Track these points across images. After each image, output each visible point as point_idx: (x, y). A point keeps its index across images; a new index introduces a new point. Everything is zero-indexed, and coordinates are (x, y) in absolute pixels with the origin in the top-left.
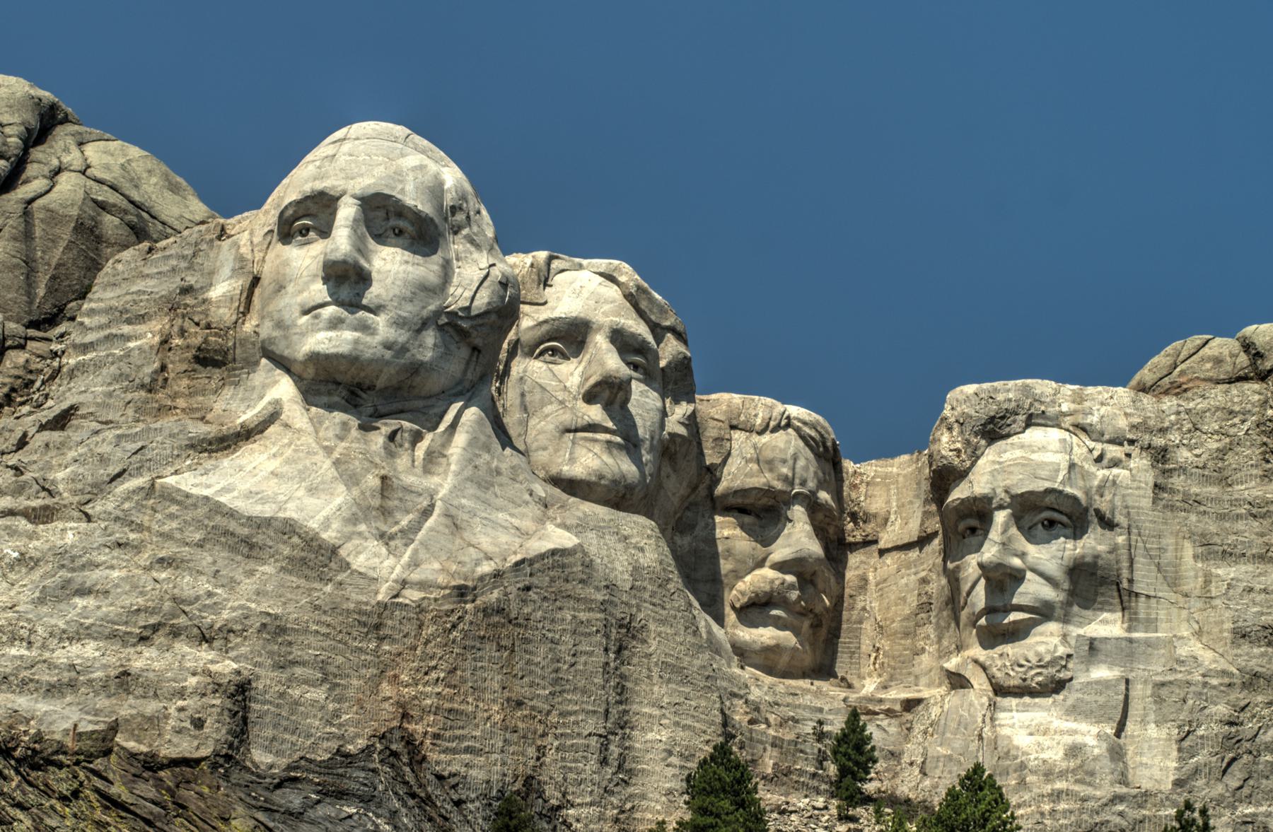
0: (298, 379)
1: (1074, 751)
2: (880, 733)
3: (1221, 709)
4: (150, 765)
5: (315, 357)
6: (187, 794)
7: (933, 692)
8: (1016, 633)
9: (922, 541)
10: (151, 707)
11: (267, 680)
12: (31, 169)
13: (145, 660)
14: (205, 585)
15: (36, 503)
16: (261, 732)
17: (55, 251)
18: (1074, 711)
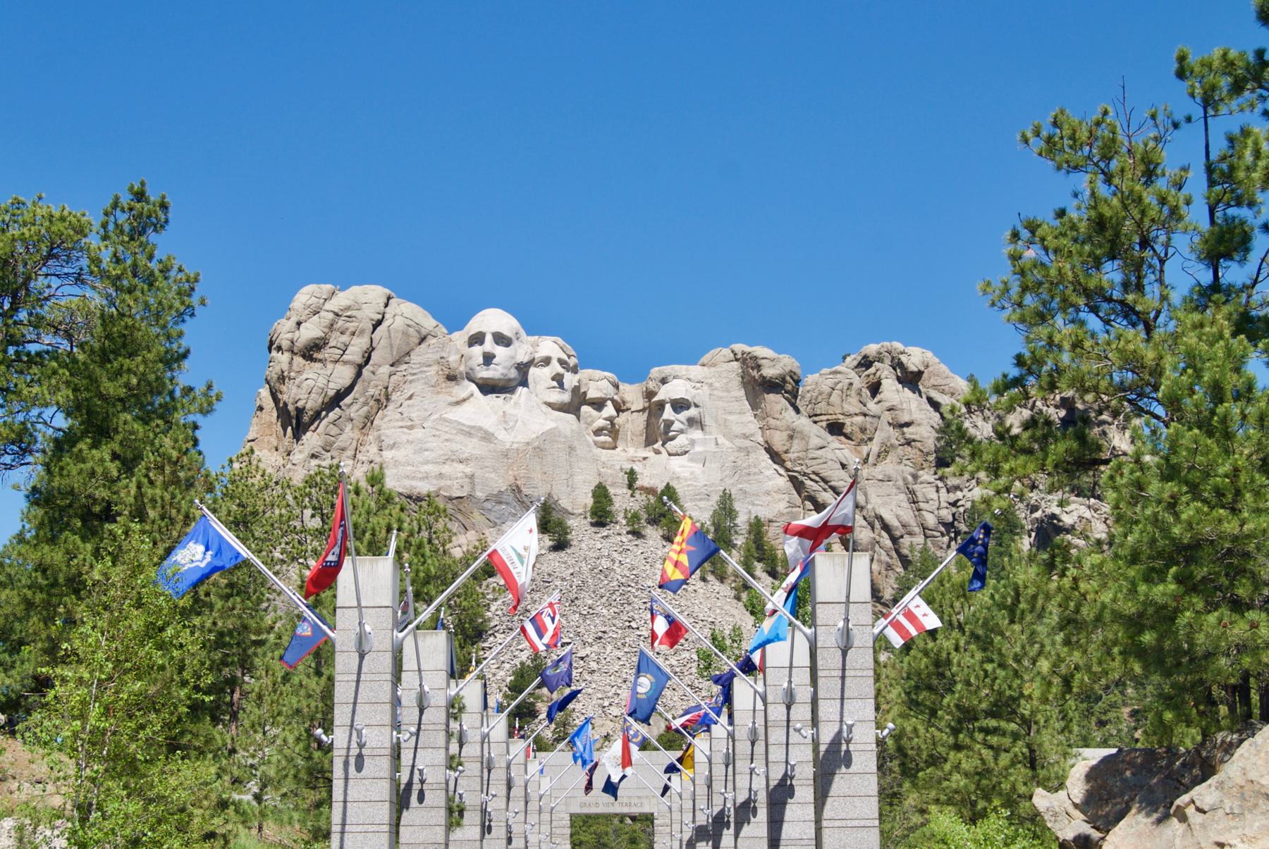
0: (477, 384)
1: (692, 473)
2: (637, 468)
3: (732, 459)
4: (451, 499)
5: (482, 378)
6: (461, 507)
7: (652, 454)
8: (673, 439)
9: (643, 410)
10: (449, 483)
11: (478, 473)
12: (387, 316)
13: (446, 469)
14: (459, 446)
15: (409, 423)
16: (478, 487)
17: (397, 342)
18: (691, 460)
